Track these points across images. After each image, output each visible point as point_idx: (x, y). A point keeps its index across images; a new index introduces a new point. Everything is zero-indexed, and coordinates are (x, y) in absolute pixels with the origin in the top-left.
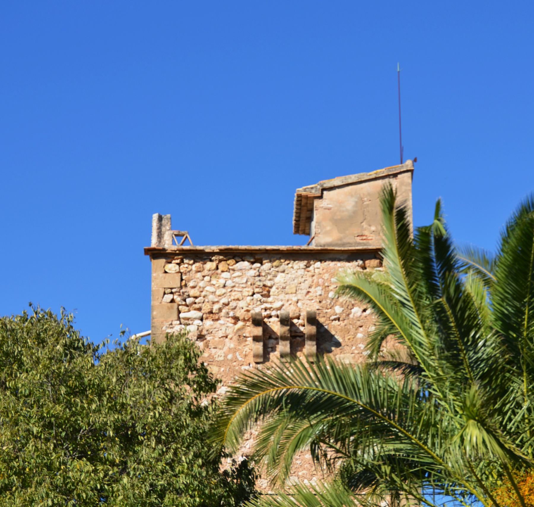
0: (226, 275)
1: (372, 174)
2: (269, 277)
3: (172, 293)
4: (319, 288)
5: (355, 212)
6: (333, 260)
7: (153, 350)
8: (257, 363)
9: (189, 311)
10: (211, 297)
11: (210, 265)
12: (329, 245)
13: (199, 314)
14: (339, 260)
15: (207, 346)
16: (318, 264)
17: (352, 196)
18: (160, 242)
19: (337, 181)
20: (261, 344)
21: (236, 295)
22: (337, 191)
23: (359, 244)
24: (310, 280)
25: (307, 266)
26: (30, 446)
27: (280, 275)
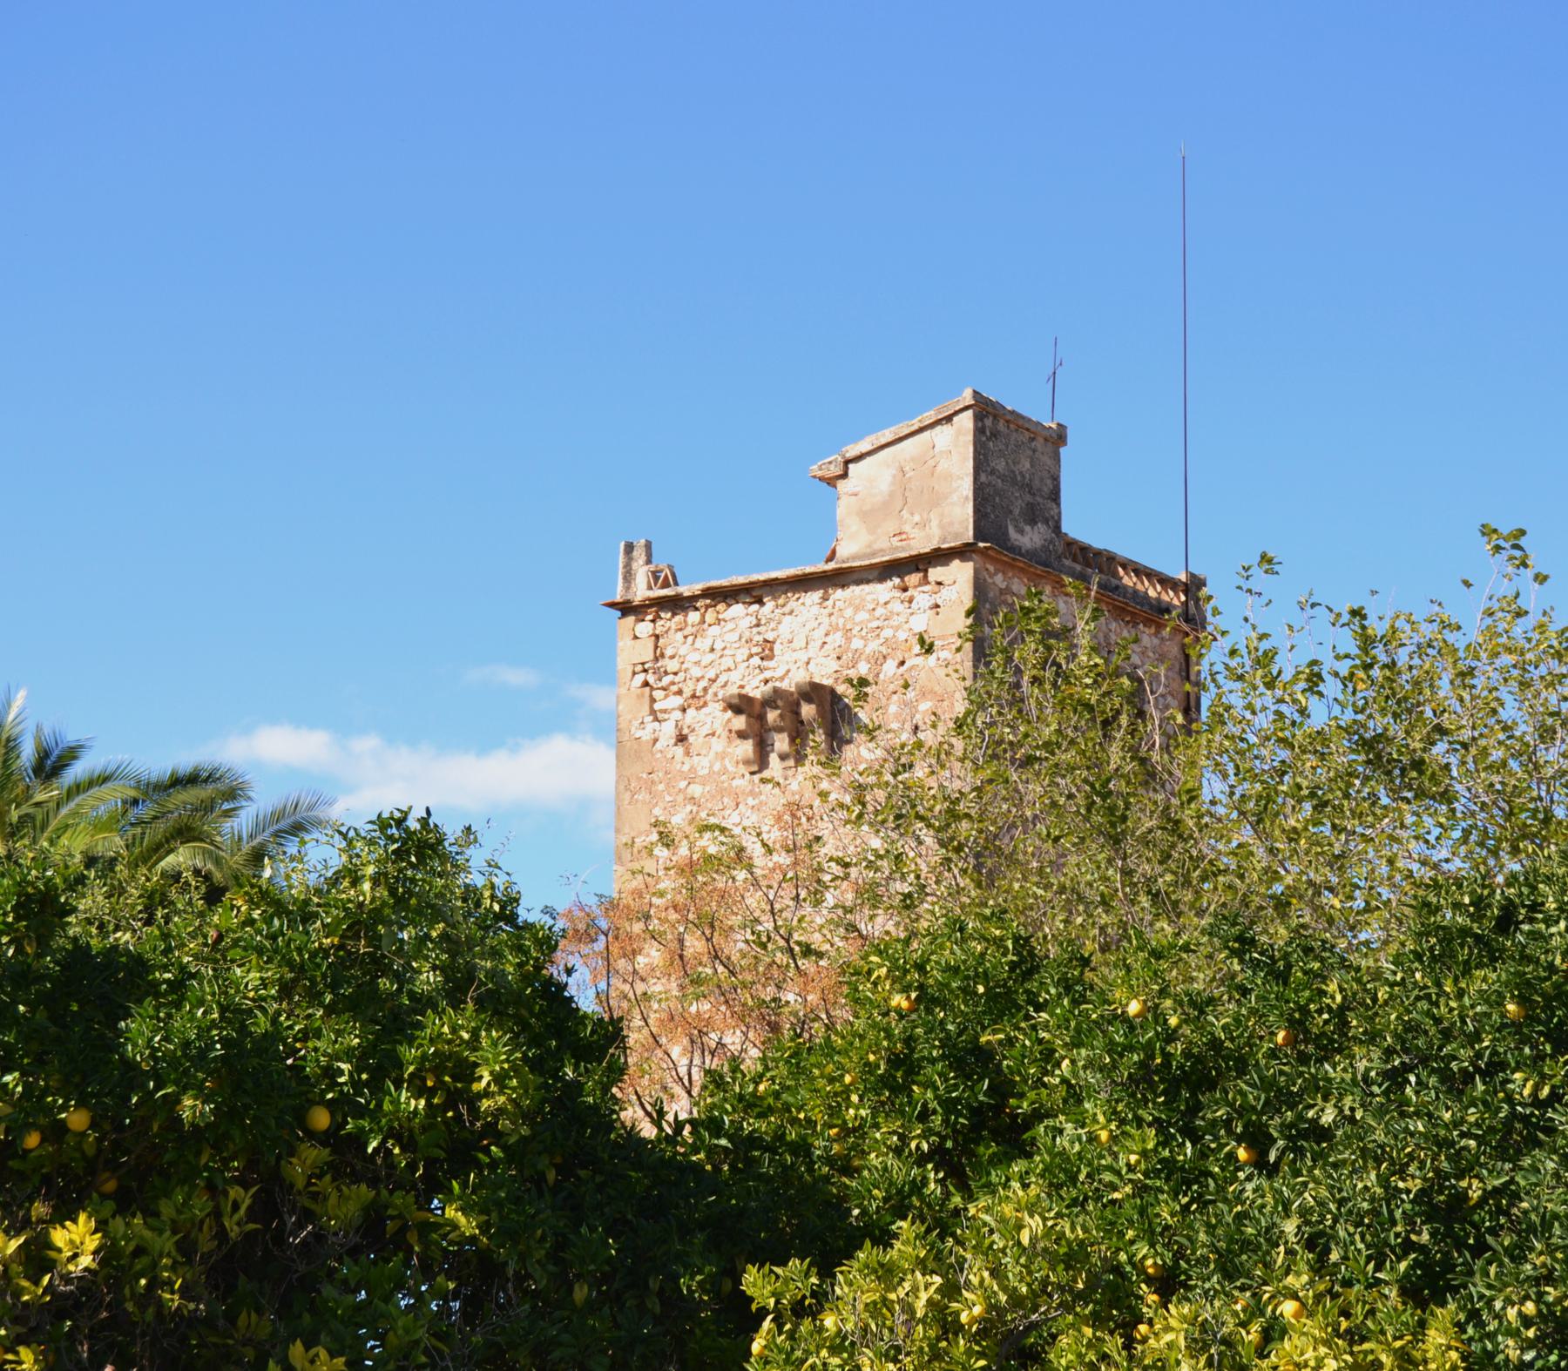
0: (715, 630)
2: (773, 625)
3: (645, 671)
4: (839, 634)
5: (892, 495)
6: (859, 582)
8: (752, 773)
9: (666, 696)
10: (696, 672)
11: (694, 617)
12: (854, 558)
13: (678, 701)
14: (868, 582)
15: (687, 753)
16: (839, 591)
18: (627, 588)
19: (864, 446)
20: (750, 742)
21: (727, 662)
22: (868, 460)
23: (903, 549)
24: (826, 620)
25: (825, 598)
27: (787, 619)
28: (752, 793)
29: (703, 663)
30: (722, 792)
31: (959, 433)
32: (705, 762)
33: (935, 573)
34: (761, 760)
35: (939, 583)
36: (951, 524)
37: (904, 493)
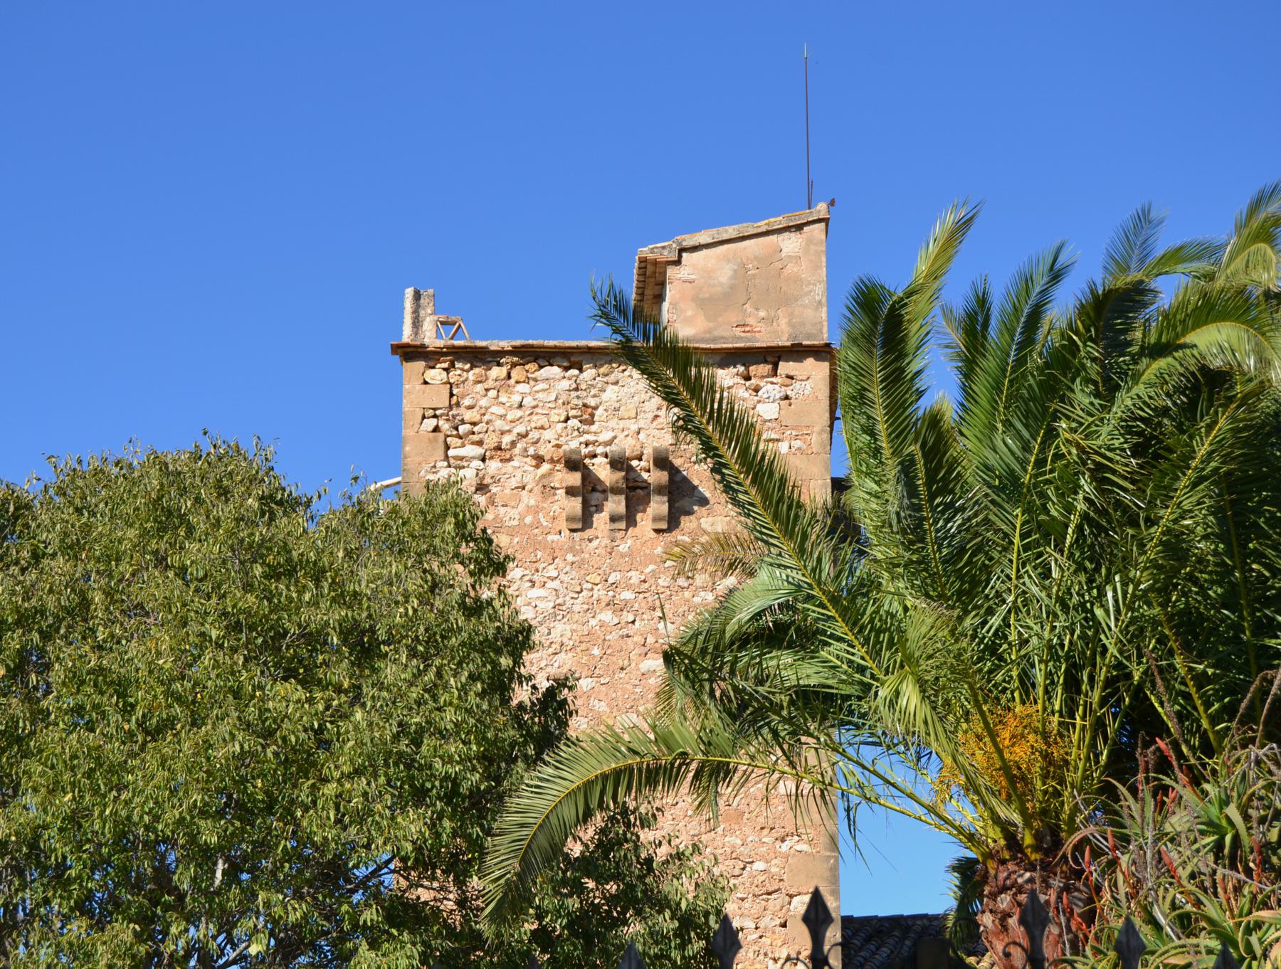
0: (523, 388)
1: (762, 226)
2: (593, 392)
3: (435, 416)
5: (732, 287)
7: (405, 508)
9: (463, 446)
10: (499, 424)
11: (496, 372)
13: (479, 451)
17: (729, 261)
19: (703, 237)
20: (580, 499)
21: (539, 420)
22: (705, 252)
23: (740, 339)
26: (207, 660)
27: (611, 389)
28: (571, 550)
29: (509, 417)
30: (535, 545)
31: (810, 241)
32: (514, 513)
33: (785, 367)
34: (586, 520)
35: (792, 378)
36: (803, 324)
37: (744, 288)
